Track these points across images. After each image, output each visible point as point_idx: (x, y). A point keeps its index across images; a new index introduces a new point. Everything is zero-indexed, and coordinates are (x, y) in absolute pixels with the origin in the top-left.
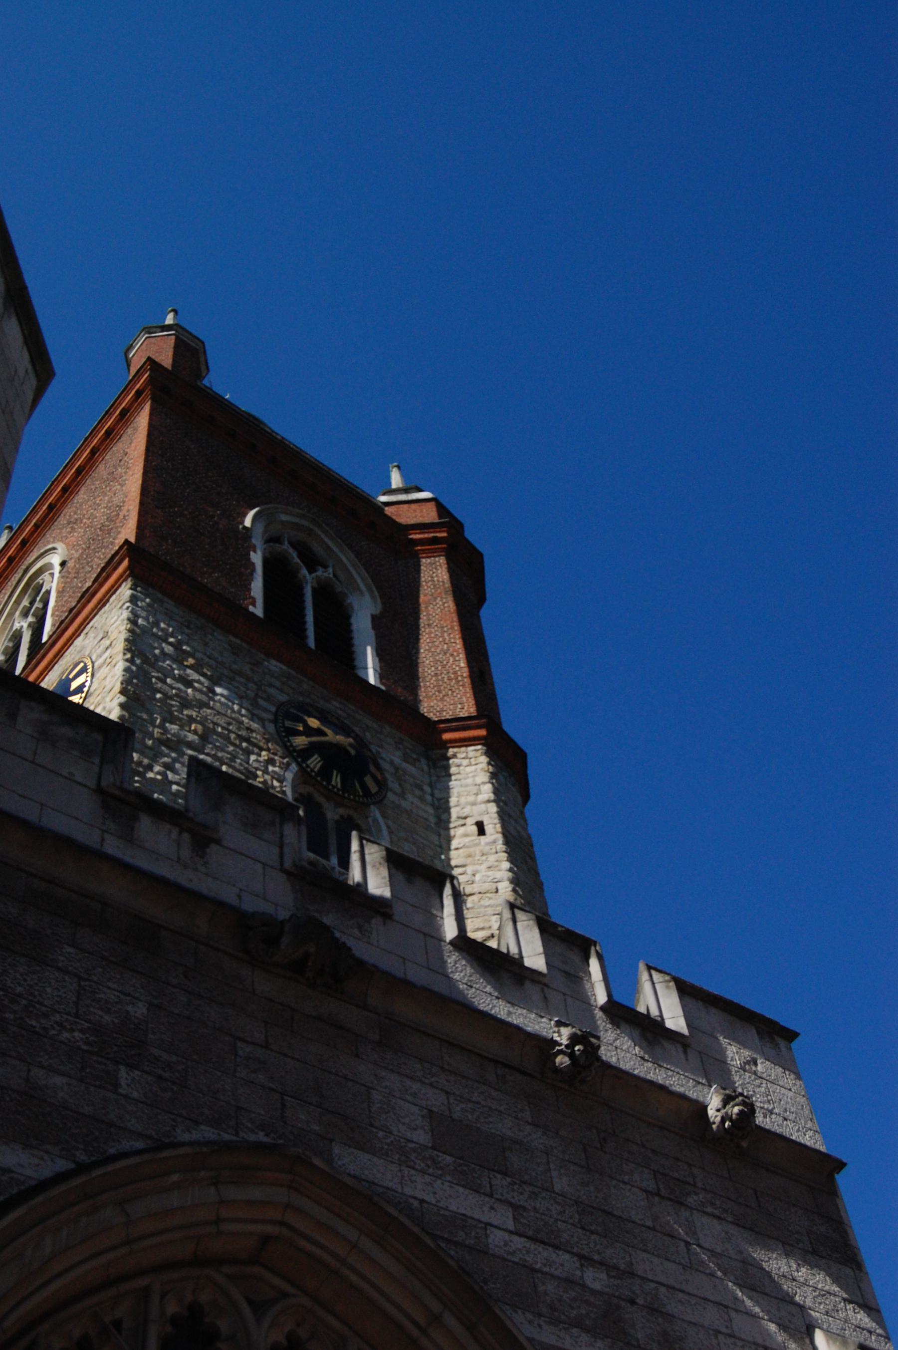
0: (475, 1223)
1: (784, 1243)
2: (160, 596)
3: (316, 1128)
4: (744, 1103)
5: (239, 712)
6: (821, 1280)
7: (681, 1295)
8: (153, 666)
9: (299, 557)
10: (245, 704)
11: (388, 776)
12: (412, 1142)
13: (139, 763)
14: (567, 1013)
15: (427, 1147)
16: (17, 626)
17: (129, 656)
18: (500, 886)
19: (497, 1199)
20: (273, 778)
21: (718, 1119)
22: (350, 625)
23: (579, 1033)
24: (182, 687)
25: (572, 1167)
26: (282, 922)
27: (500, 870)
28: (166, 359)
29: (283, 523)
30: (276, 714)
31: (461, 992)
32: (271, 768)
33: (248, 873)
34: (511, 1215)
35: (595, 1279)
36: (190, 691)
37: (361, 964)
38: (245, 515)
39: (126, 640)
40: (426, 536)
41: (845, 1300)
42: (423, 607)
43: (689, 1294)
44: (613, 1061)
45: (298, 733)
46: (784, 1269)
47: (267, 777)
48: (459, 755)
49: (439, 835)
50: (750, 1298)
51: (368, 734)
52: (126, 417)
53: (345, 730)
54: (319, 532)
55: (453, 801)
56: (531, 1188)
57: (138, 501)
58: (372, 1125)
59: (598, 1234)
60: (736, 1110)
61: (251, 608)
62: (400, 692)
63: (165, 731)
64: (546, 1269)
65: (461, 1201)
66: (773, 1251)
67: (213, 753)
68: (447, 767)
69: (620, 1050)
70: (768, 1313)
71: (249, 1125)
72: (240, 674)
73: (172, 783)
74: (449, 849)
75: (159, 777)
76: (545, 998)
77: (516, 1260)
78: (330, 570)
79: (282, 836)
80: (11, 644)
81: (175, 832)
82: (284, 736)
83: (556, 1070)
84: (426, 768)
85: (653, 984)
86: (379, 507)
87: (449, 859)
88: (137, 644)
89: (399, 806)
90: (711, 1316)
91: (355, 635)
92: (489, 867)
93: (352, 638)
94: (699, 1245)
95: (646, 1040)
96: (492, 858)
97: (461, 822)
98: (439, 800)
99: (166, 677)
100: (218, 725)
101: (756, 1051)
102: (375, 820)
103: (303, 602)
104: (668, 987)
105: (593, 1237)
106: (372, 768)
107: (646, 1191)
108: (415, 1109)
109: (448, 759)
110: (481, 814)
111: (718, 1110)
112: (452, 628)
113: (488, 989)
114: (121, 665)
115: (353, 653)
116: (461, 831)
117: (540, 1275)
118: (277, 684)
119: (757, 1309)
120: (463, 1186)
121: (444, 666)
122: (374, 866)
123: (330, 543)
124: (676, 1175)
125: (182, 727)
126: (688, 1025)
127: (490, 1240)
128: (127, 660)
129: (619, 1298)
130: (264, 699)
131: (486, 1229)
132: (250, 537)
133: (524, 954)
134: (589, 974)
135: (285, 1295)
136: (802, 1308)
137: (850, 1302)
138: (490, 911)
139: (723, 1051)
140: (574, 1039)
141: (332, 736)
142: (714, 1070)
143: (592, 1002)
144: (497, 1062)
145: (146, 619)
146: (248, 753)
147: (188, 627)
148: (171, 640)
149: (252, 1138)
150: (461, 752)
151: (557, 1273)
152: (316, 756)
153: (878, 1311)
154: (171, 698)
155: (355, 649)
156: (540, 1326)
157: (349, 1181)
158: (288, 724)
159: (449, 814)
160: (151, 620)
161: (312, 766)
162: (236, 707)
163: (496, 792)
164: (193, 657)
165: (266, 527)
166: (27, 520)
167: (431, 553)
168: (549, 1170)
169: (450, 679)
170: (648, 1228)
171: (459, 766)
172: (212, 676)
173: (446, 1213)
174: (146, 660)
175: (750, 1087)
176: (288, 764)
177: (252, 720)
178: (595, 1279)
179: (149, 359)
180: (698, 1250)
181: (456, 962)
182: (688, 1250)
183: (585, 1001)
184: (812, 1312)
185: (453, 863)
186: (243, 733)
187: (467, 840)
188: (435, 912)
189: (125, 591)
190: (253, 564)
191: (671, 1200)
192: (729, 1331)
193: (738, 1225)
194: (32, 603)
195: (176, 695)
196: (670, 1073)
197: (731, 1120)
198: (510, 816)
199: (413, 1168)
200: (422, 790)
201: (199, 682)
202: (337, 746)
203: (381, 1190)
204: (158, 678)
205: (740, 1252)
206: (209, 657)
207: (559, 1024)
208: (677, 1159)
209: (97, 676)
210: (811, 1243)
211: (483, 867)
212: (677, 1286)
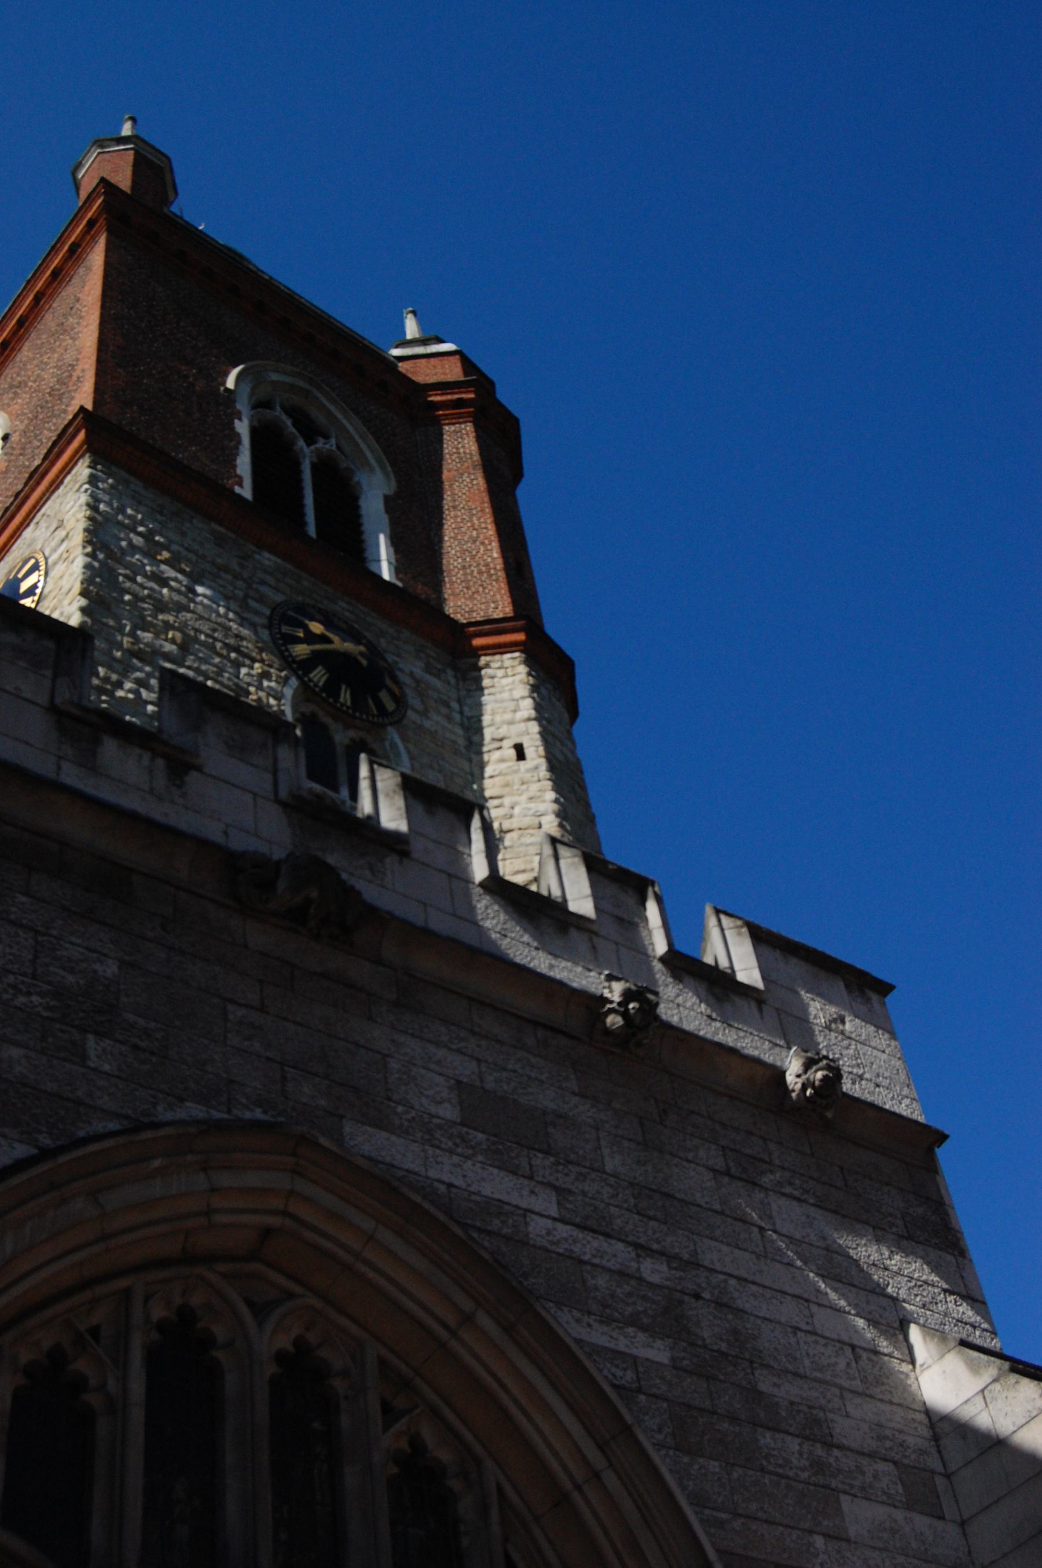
1: (874, 1228)
2: (124, 474)
3: (323, 1102)
4: (828, 1068)
5: (226, 616)
6: (918, 1269)
7: (754, 1288)
8: (120, 561)
9: (294, 425)
10: (233, 605)
11: (408, 691)
12: (438, 1117)
13: (106, 680)
15: (454, 1123)
17: (89, 549)
19: (541, 1183)
20: (269, 695)
21: (799, 1086)
22: (357, 508)
23: (633, 988)
25: (626, 1144)
26: (278, 863)
27: (544, 801)
28: (124, 180)
29: (273, 382)
30: (270, 618)
31: (493, 943)
32: (266, 683)
33: (237, 806)
34: (554, 1198)
36: (165, 591)
37: (373, 911)
38: (226, 374)
39: (85, 530)
40: (449, 397)
41: (945, 1291)
43: (764, 1286)
44: (675, 1020)
45: (298, 641)
46: (875, 1256)
47: (262, 694)
48: (493, 665)
49: (470, 761)
50: (835, 1290)
51: (382, 640)
52: (76, 253)
53: (356, 637)
54: (319, 395)
55: (486, 719)
57: (94, 358)
58: (389, 1099)
60: (819, 1075)
61: (237, 489)
62: (420, 590)
63: (137, 640)
64: (596, 1261)
65: (497, 1185)
66: (862, 1236)
67: (196, 665)
68: (479, 679)
69: (683, 1008)
70: (856, 1306)
71: (244, 1101)
72: (226, 569)
74: (482, 778)
75: (131, 696)
76: (594, 947)
77: (561, 1251)
78: (333, 441)
79: (276, 761)
81: (146, 757)
82: (280, 645)
83: (607, 1032)
84: (453, 681)
85: (722, 930)
86: (392, 362)
87: (482, 790)
88: (99, 534)
89: (421, 727)
90: (788, 1311)
91: (365, 520)
92: (531, 798)
93: (360, 525)
94: (775, 1231)
96: (534, 788)
97: (496, 745)
98: (469, 718)
99: (136, 574)
100: (201, 632)
102: (393, 745)
103: (300, 481)
104: (739, 934)
105: (652, 1223)
106: (388, 682)
107: (714, 1170)
108: (440, 1080)
109: (480, 669)
111: (798, 1076)
112: (482, 510)
113: (526, 938)
114: (80, 561)
115: (362, 542)
116: (496, 755)
117: (589, 1267)
119: (843, 1303)
120: (499, 1168)
121: (473, 557)
122: (387, 795)
123: (332, 408)
124: (748, 1151)
125: (157, 635)
126: (764, 978)
127: (530, 1229)
128: (87, 555)
129: (682, 1292)
130: (257, 601)
131: (525, 1216)
133: (569, 897)
134: (646, 920)
135: (291, 1295)
136: (895, 1300)
137: (952, 1293)
139: (805, 1008)
140: (628, 996)
141: (339, 644)
142: (795, 1029)
143: (650, 952)
144: (536, 1024)
145: (109, 504)
146: (237, 665)
147: (161, 513)
148: (141, 529)
149: (248, 1115)
150: (496, 661)
151: (609, 1265)
152: (320, 668)
153: (984, 1303)
154: (143, 600)
155: (365, 537)
156: (589, 1325)
158: (285, 629)
159: (482, 735)
160: (115, 505)
161: (315, 679)
162: (222, 610)
163: (538, 707)
164: (167, 548)
167: (456, 419)
168: (599, 1148)
169: (480, 572)
170: (716, 1212)
171: (492, 677)
172: (191, 572)
173: (478, 1198)
174: (110, 555)
175: (837, 1049)
176: (286, 679)
179: (103, 180)
180: (775, 1236)
181: (487, 908)
182: (763, 1236)
183: (640, 950)
184: (906, 1305)
185: (487, 794)
186: (231, 641)
187: (503, 766)
188: (461, 848)
189: (82, 470)
190: (238, 435)
191: (741, 1179)
192: (809, 1328)
195: (149, 596)
196: (742, 1034)
197: (813, 1087)
199: (439, 1148)
200: (449, 707)
201: (176, 580)
202: (345, 655)
203: (401, 1173)
204: (125, 576)
205: (824, 1238)
207: (610, 978)
209: (54, 573)
210: (906, 1227)
211: (524, 798)
212: (750, 1278)
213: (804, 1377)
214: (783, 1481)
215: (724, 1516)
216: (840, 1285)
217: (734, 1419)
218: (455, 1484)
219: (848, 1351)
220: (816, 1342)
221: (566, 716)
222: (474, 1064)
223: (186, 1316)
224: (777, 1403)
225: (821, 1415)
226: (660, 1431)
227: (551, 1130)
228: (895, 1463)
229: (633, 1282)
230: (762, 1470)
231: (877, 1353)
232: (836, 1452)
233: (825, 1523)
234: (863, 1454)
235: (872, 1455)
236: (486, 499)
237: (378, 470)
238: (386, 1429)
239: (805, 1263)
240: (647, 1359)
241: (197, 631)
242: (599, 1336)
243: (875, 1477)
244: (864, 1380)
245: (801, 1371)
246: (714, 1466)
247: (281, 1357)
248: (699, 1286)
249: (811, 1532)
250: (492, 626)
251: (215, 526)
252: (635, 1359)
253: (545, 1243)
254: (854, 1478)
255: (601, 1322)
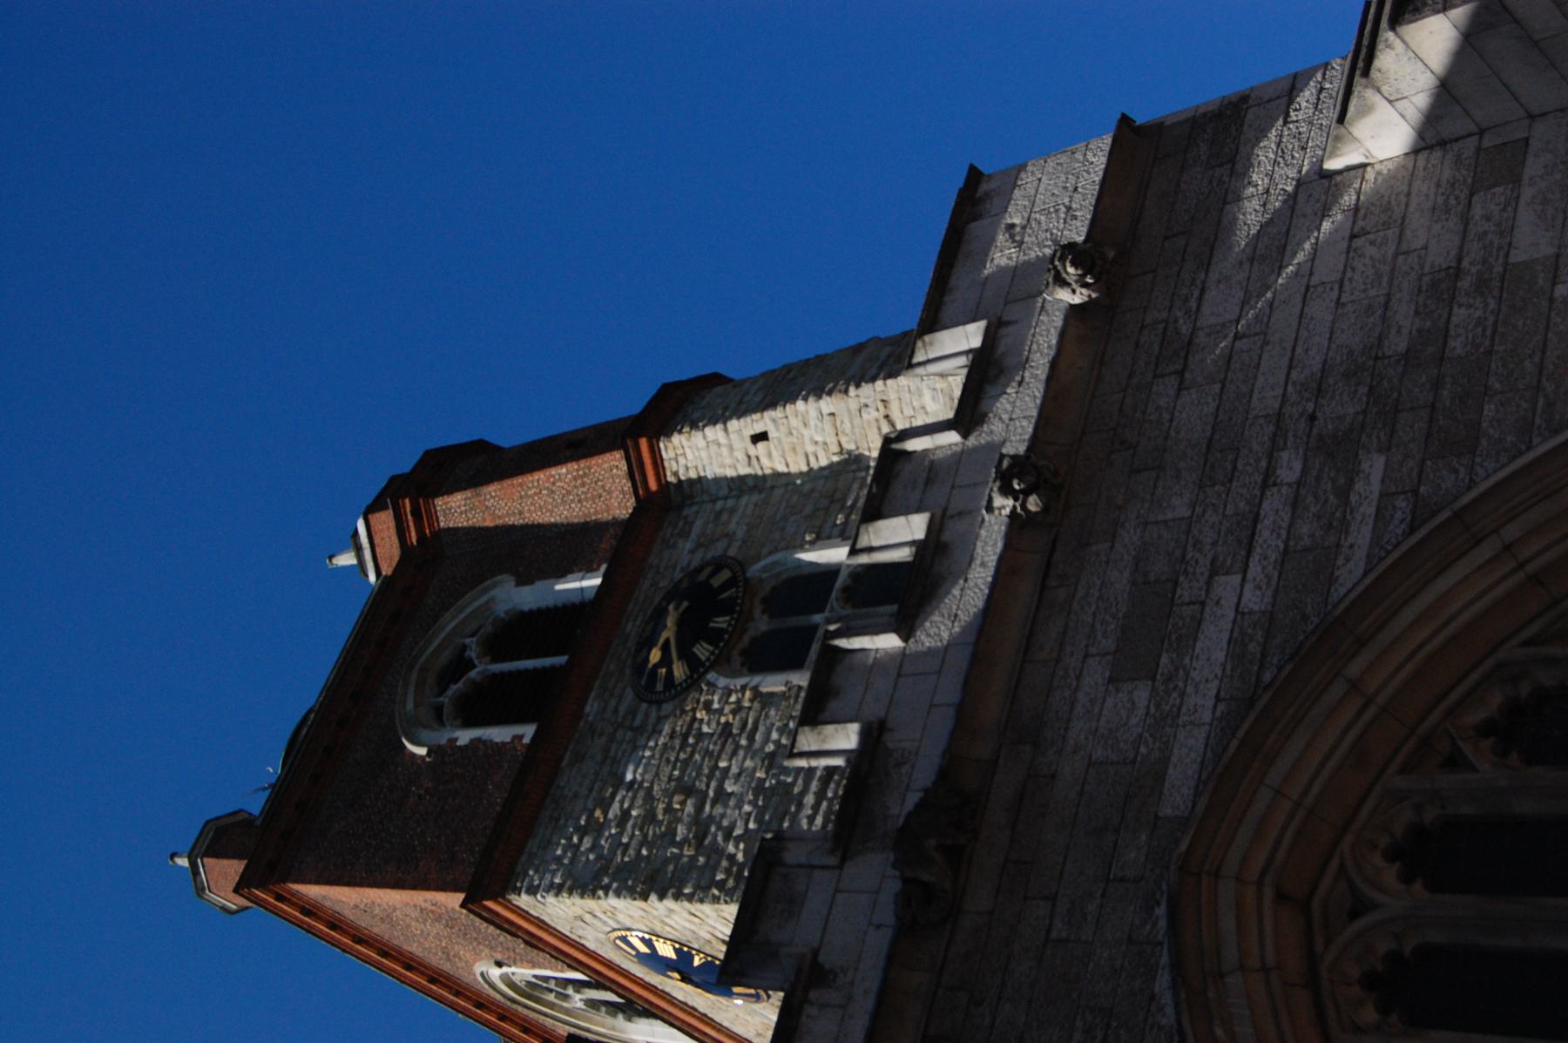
0: (1237, 630)
1: (1225, 203)
2: (524, 858)
3: (1144, 837)
4: (1062, 259)
5: (653, 749)
6: (1265, 153)
7: (1299, 350)
8: (610, 861)
9: (456, 682)
10: (641, 742)
11: (709, 556)
12: (1148, 707)
13: (728, 871)
14: (976, 485)
15: (1154, 689)
16: (580, 1005)
17: (601, 893)
18: (826, 411)
19: (1207, 592)
20: (727, 702)
21: (1084, 291)
22: (531, 612)
23: (998, 484)
24: (630, 823)
25: (1160, 490)
26: (905, 881)
28: (233, 868)
29: (416, 705)
30: (650, 702)
31: (964, 630)
32: (716, 706)
34: (1223, 578)
35: (1289, 467)
36: (634, 813)
37: (943, 775)
38: (413, 755)
39: (582, 897)
40: (411, 524)
41: (1286, 122)
42: (499, 522)
43: (1296, 339)
44: (1029, 428)
45: (670, 673)
46: (1255, 204)
47: (727, 709)
49: (773, 487)
50: (1294, 254)
51: (661, 584)
52: (311, 909)
53: (659, 615)
54: (423, 659)
55: (730, 473)
56: (1190, 549)
57: (412, 892)
58: (1134, 762)
59: (1236, 460)
60: (1071, 270)
61: (526, 740)
62: (607, 544)
63: (685, 840)
64: (1284, 533)
65: (1213, 643)
66: (1236, 219)
68: (690, 481)
69: (1014, 418)
70: (1310, 231)
71: (1148, 927)
72: (606, 750)
73: (746, 829)
74: (789, 474)
75: (742, 846)
76: (960, 514)
77: (1276, 574)
78: (468, 641)
79: (800, 866)
80: (603, 1009)
81: (810, 1010)
82: (676, 692)
83: (1046, 509)
84: (695, 508)
85: (929, 361)
87: (801, 473)
88: (586, 884)
89: (744, 541)
90: (1320, 310)
91: (543, 604)
93: (548, 608)
94: (1238, 322)
95: (997, 377)
96: (794, 422)
97: (754, 461)
98: (731, 490)
99: (621, 844)
101: (999, 223)
102: (765, 569)
103: (510, 673)
104: (931, 344)
105: (1240, 467)
106: (702, 577)
107: (1179, 390)
108: (1109, 702)
109: (680, 481)
110: (742, 437)
111: (1074, 292)
112: (521, 485)
113: (956, 592)
114: (613, 901)
115: (564, 606)
116: (765, 461)
117: (1292, 543)
118: (613, 702)
119: (1307, 246)
120: (1195, 640)
121: (569, 493)
122: (824, 741)
124: (1156, 348)
125: (679, 820)
126: (974, 320)
127: (1256, 608)
128: (606, 895)
129: (1309, 436)
131: (1243, 614)
132: (440, 747)
133: (909, 539)
134: (925, 451)
135: (1342, 867)
136: (1300, 183)
137: (1287, 115)
138: (857, 421)
139: (1002, 270)
140: (1006, 490)
141: (669, 632)
142: (1022, 287)
143: (958, 449)
144: (1043, 587)
145: (554, 873)
146: (700, 736)
147: (558, 820)
148: (575, 840)
149: (1163, 923)
150: (671, 466)
151: (1287, 518)
153: (1295, 76)
154: (645, 836)
155: (559, 604)
156: (1352, 546)
157: (1202, 803)
158: (659, 687)
159: (746, 476)
160: (554, 867)
162: (647, 753)
163: (713, 422)
164: (592, 812)
165: (425, 727)
166: (452, 1005)
167: (432, 516)
168: (1166, 522)
169: (583, 485)
170: (1222, 390)
171: (687, 468)
173: (1229, 666)
174: (603, 871)
175: (1042, 236)
176: (709, 684)
177: (660, 732)
178: (1289, 467)
179: (236, 891)
180: (1243, 322)
181: (928, 635)
182: (1244, 336)
183: (959, 458)
184: (1305, 169)
185: (805, 469)
186: (677, 742)
187: (775, 454)
188: (871, 661)
189: (523, 900)
190: (473, 741)
191: (1186, 357)
192: (1336, 287)
193: (1209, 264)
194: (551, 991)
195: (641, 830)
196: (1035, 347)
197: (1083, 276)
198: (740, 402)
199: (1179, 709)
200: (721, 512)
201: (622, 802)
202: (680, 624)
203: (1209, 754)
204: (624, 855)
205: (1241, 263)
206: (591, 790)
207: (990, 508)
208: (1137, 345)
209: (628, 924)
210: (1221, 165)
211: (805, 432)
212: (1289, 354)
213: (1389, 296)
214: (1501, 329)
215: (1541, 401)
216: (1289, 248)
217: (1437, 384)
218: (1525, 689)
219: (1358, 242)
220: (1350, 279)
221: (719, 389)
222: (1090, 661)
223: (1370, 982)
224: (1419, 331)
225: (1426, 279)
226: (1456, 471)
227: (1152, 577)
228: (1472, 195)
229: (1303, 492)
230: (1490, 352)
231: (1357, 209)
232: (1465, 264)
233: (1541, 282)
234: (1465, 231)
235: (1466, 221)
236: (509, 482)
237: (493, 593)
238: (1475, 770)
239: (1268, 288)
240: (1383, 481)
241: (670, 779)
242: (1361, 536)
243: (1488, 219)
244: (1386, 225)
245: (1382, 299)
246: (1489, 410)
247: (1407, 878)
248: (1302, 415)
249: (1551, 300)
250: (635, 472)
251: (564, 763)
252: (1382, 495)
253: (1269, 593)
254: (1491, 243)
255: (1347, 533)
